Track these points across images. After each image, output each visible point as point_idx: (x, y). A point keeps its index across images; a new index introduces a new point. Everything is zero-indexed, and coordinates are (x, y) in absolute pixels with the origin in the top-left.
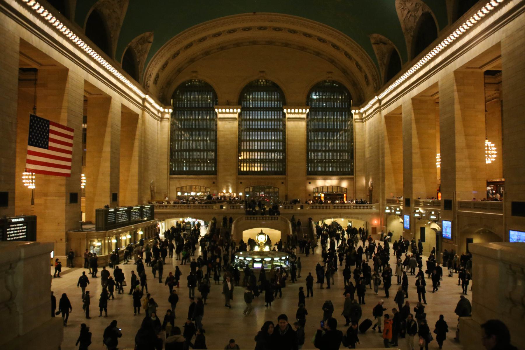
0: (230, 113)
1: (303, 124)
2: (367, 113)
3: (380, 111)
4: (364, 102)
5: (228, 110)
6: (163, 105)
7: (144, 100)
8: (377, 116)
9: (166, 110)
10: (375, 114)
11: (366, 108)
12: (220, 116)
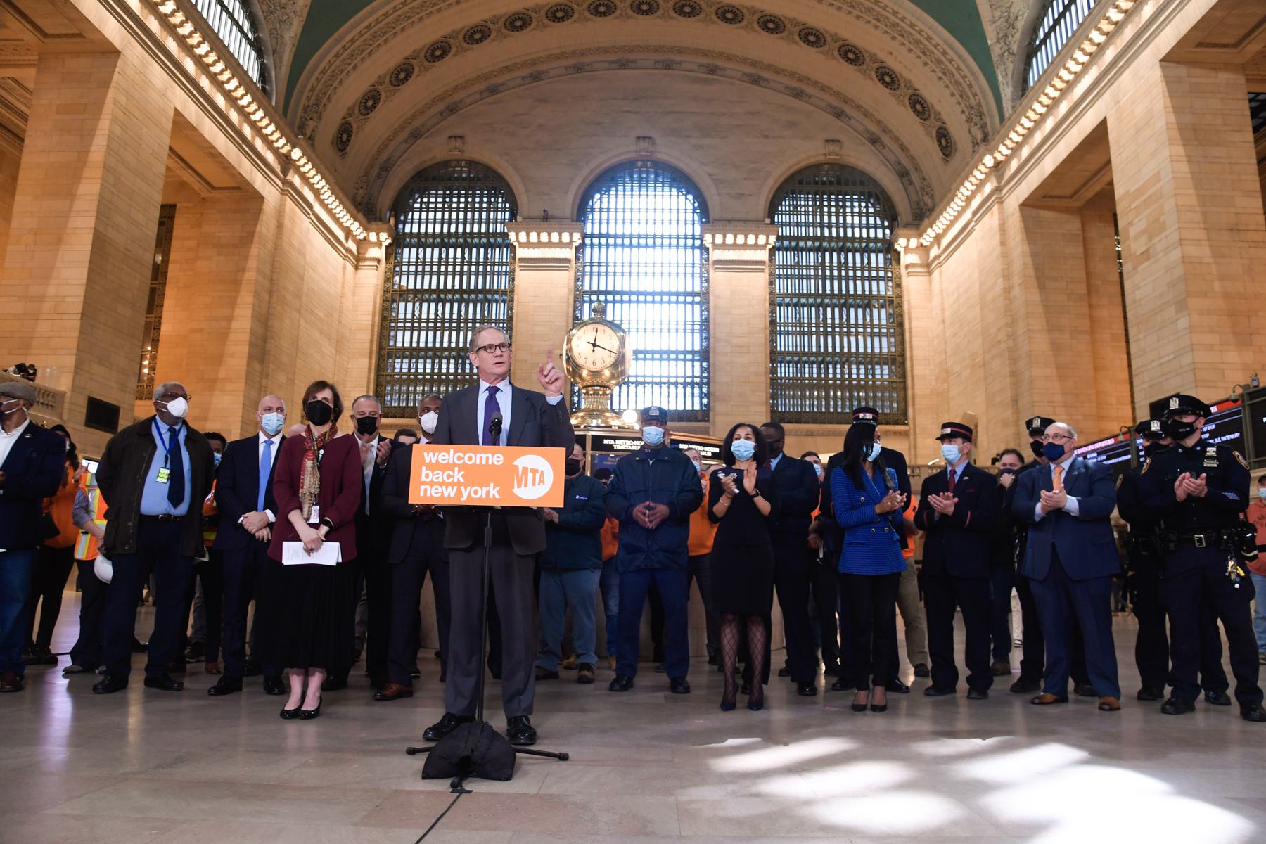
0: (550, 244)
1: (761, 279)
2: (945, 242)
3: (1001, 201)
4: (931, 210)
5: (544, 237)
6: (360, 216)
7: (287, 162)
8: (991, 220)
9: (373, 237)
10: (977, 222)
11: (939, 227)
12: (521, 253)
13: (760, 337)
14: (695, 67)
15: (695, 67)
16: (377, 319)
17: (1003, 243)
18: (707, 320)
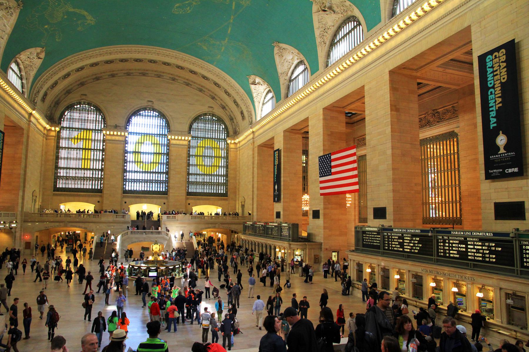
2: (242, 143)
3: (254, 142)
5: (115, 133)
6: (50, 123)
7: (31, 114)
9: (53, 129)
11: (241, 139)
13: (184, 170)
14: (168, 78)
15: (168, 78)
16: (55, 158)
17: (253, 154)
18: (168, 162)
